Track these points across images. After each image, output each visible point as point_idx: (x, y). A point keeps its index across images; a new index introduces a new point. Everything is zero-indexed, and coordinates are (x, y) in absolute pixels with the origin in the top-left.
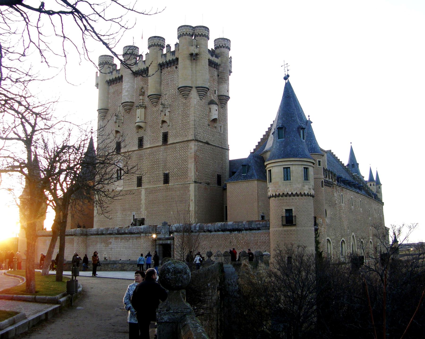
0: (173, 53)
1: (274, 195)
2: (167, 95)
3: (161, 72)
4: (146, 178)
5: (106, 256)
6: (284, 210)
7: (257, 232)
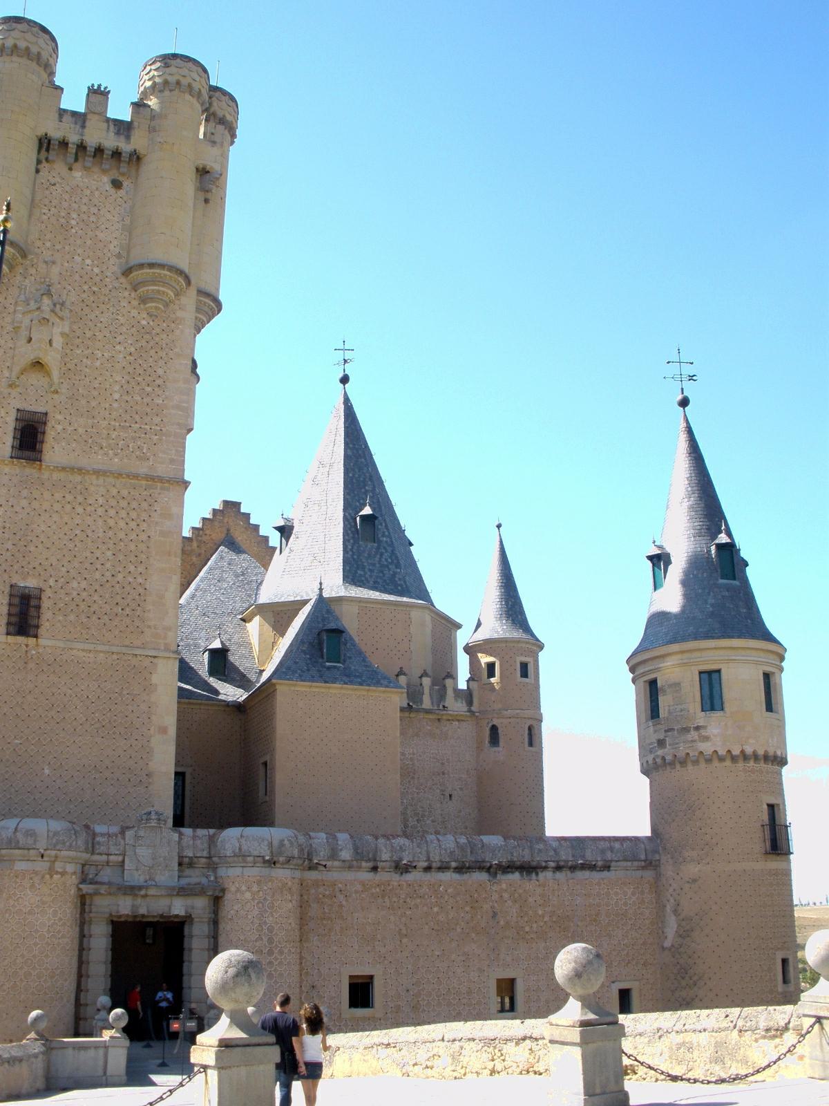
0: (123, 128)
1: (736, 752)
2: (55, 270)
3: (37, 171)
6: (766, 807)
7: (596, 875)
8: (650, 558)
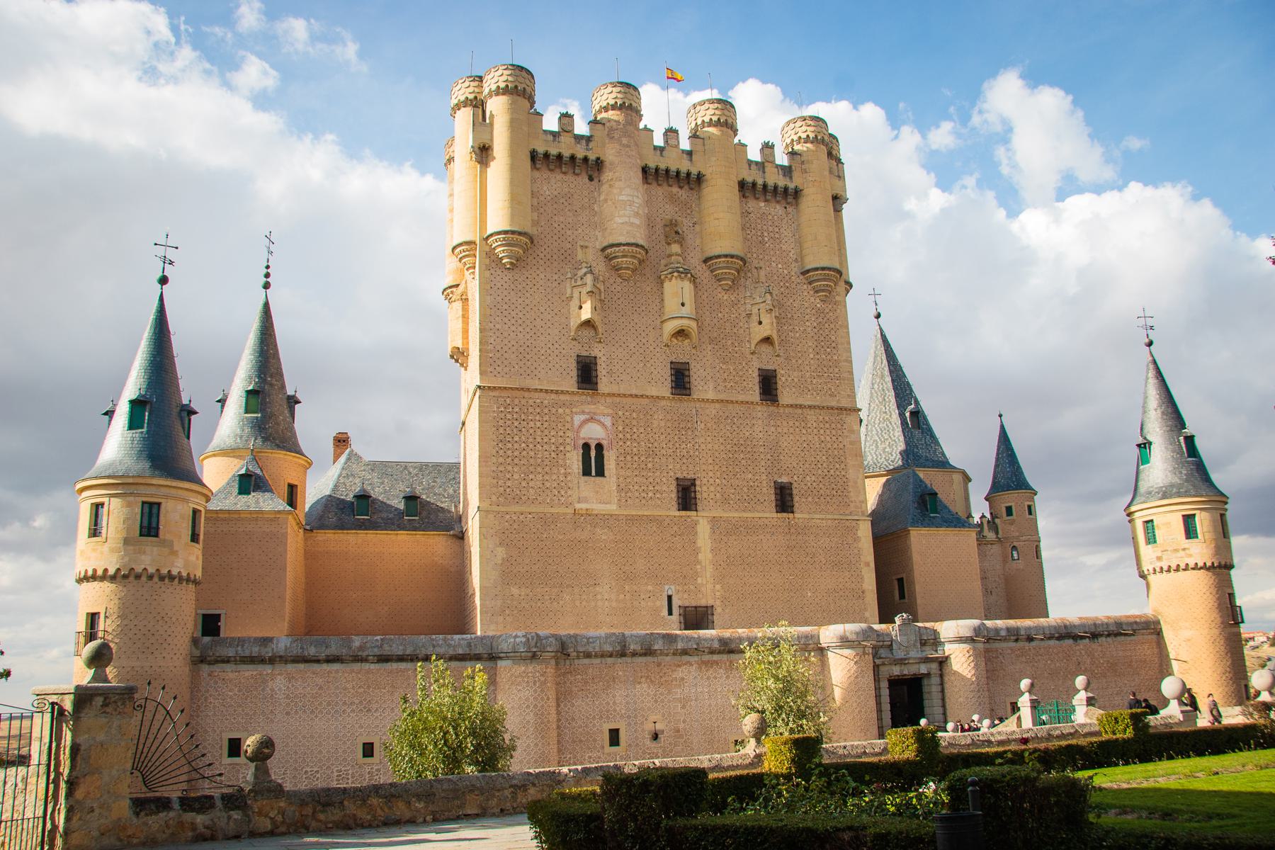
0: (787, 171)
2: (762, 273)
4: (712, 489)
5: (659, 727)
8: (1139, 446)
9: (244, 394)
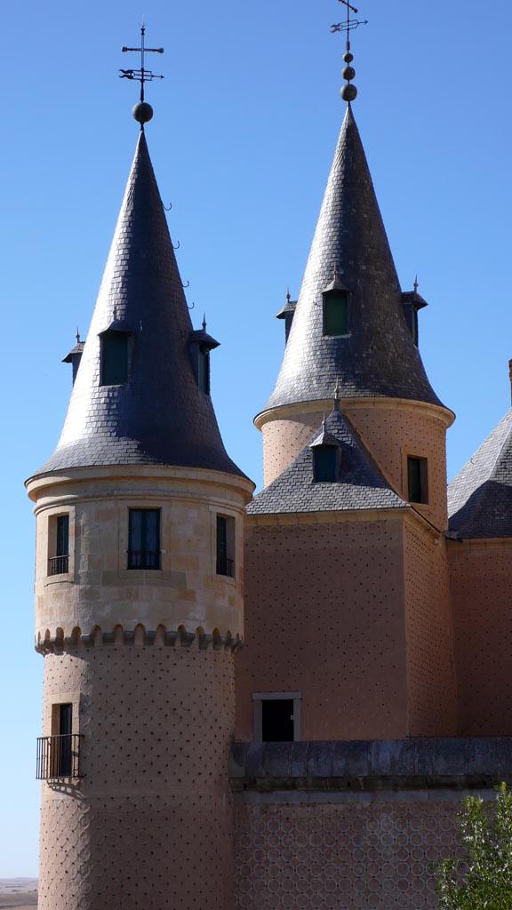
9: (320, 299)
